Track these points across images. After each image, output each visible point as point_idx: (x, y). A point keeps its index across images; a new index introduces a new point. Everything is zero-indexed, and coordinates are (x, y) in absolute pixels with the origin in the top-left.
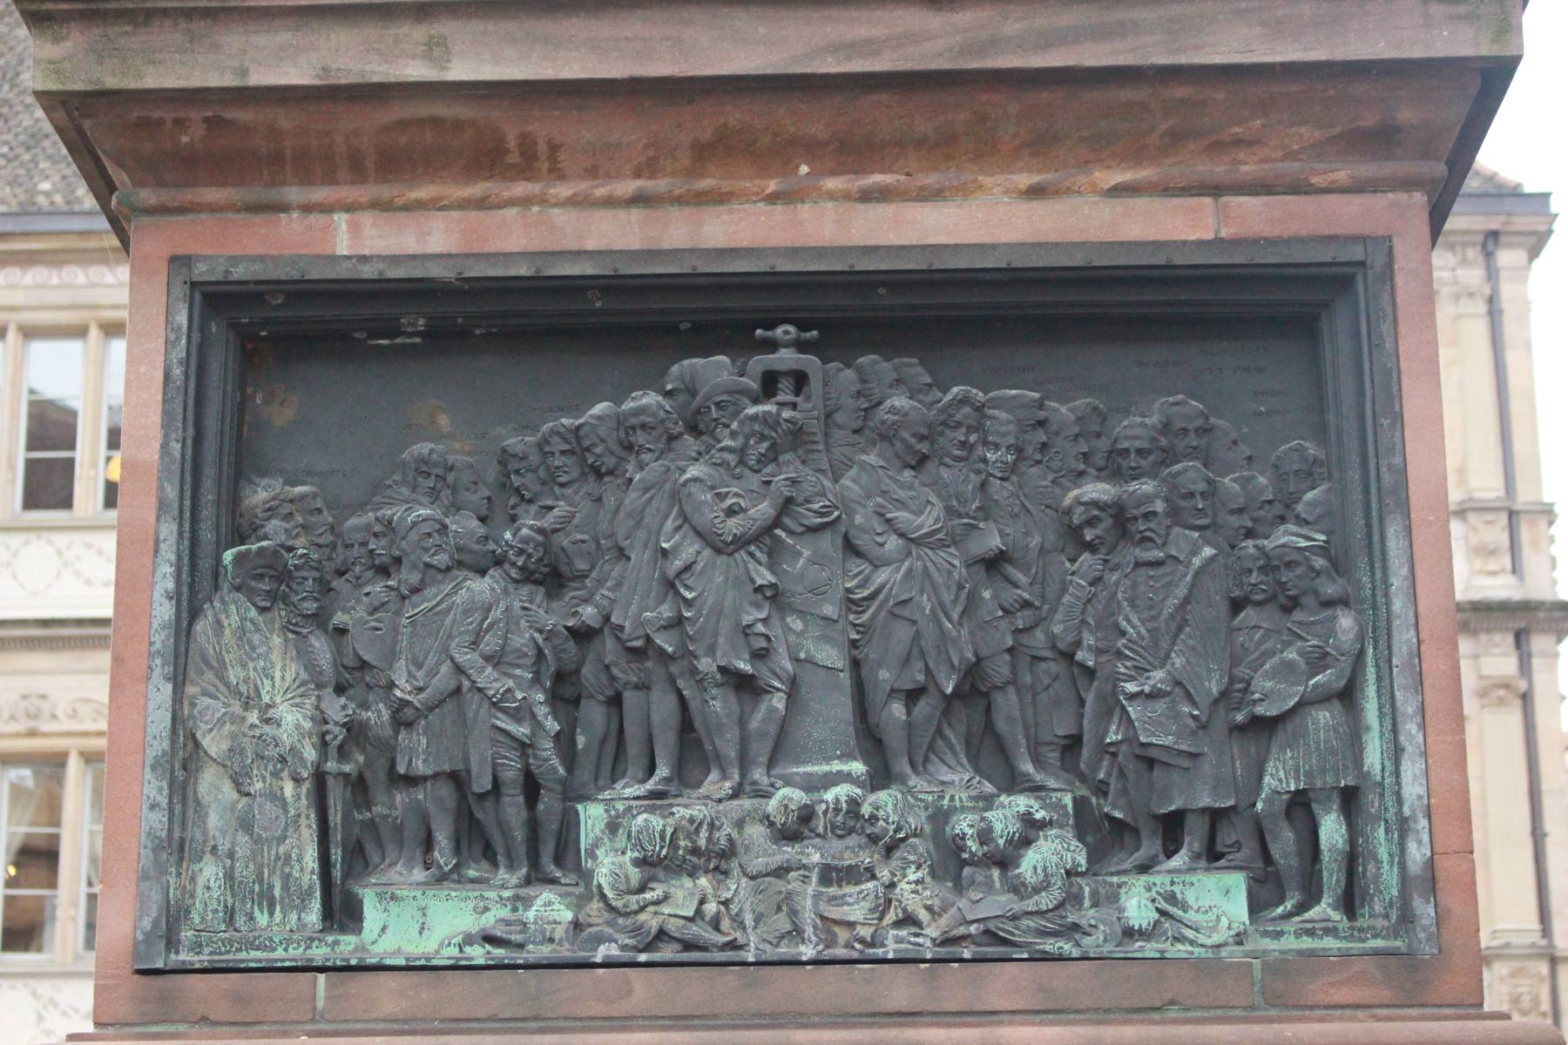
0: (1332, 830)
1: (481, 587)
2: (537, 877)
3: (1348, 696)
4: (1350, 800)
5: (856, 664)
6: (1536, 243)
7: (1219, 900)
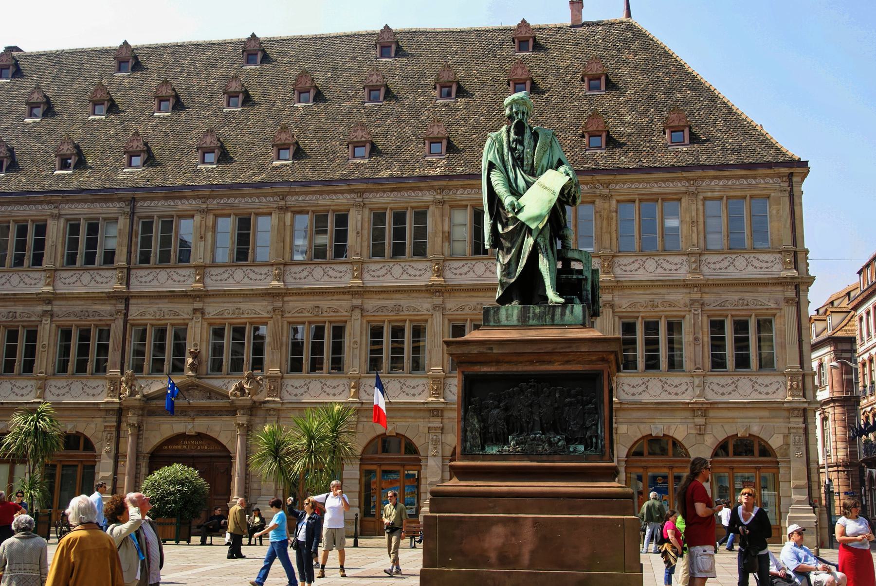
0: (594, 440)
1: (498, 410)
2: (505, 444)
3: (596, 425)
4: (597, 437)
5: (541, 419)
6: (805, 175)
7: (581, 448)
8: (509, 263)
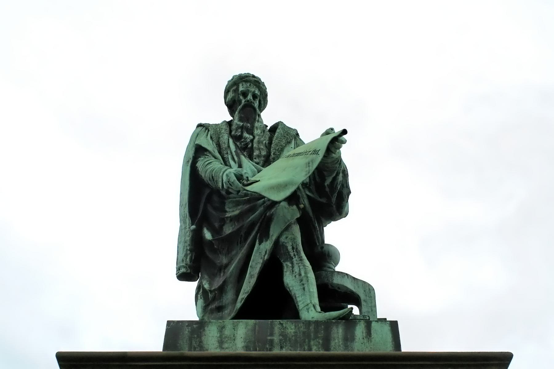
8: (222, 289)
